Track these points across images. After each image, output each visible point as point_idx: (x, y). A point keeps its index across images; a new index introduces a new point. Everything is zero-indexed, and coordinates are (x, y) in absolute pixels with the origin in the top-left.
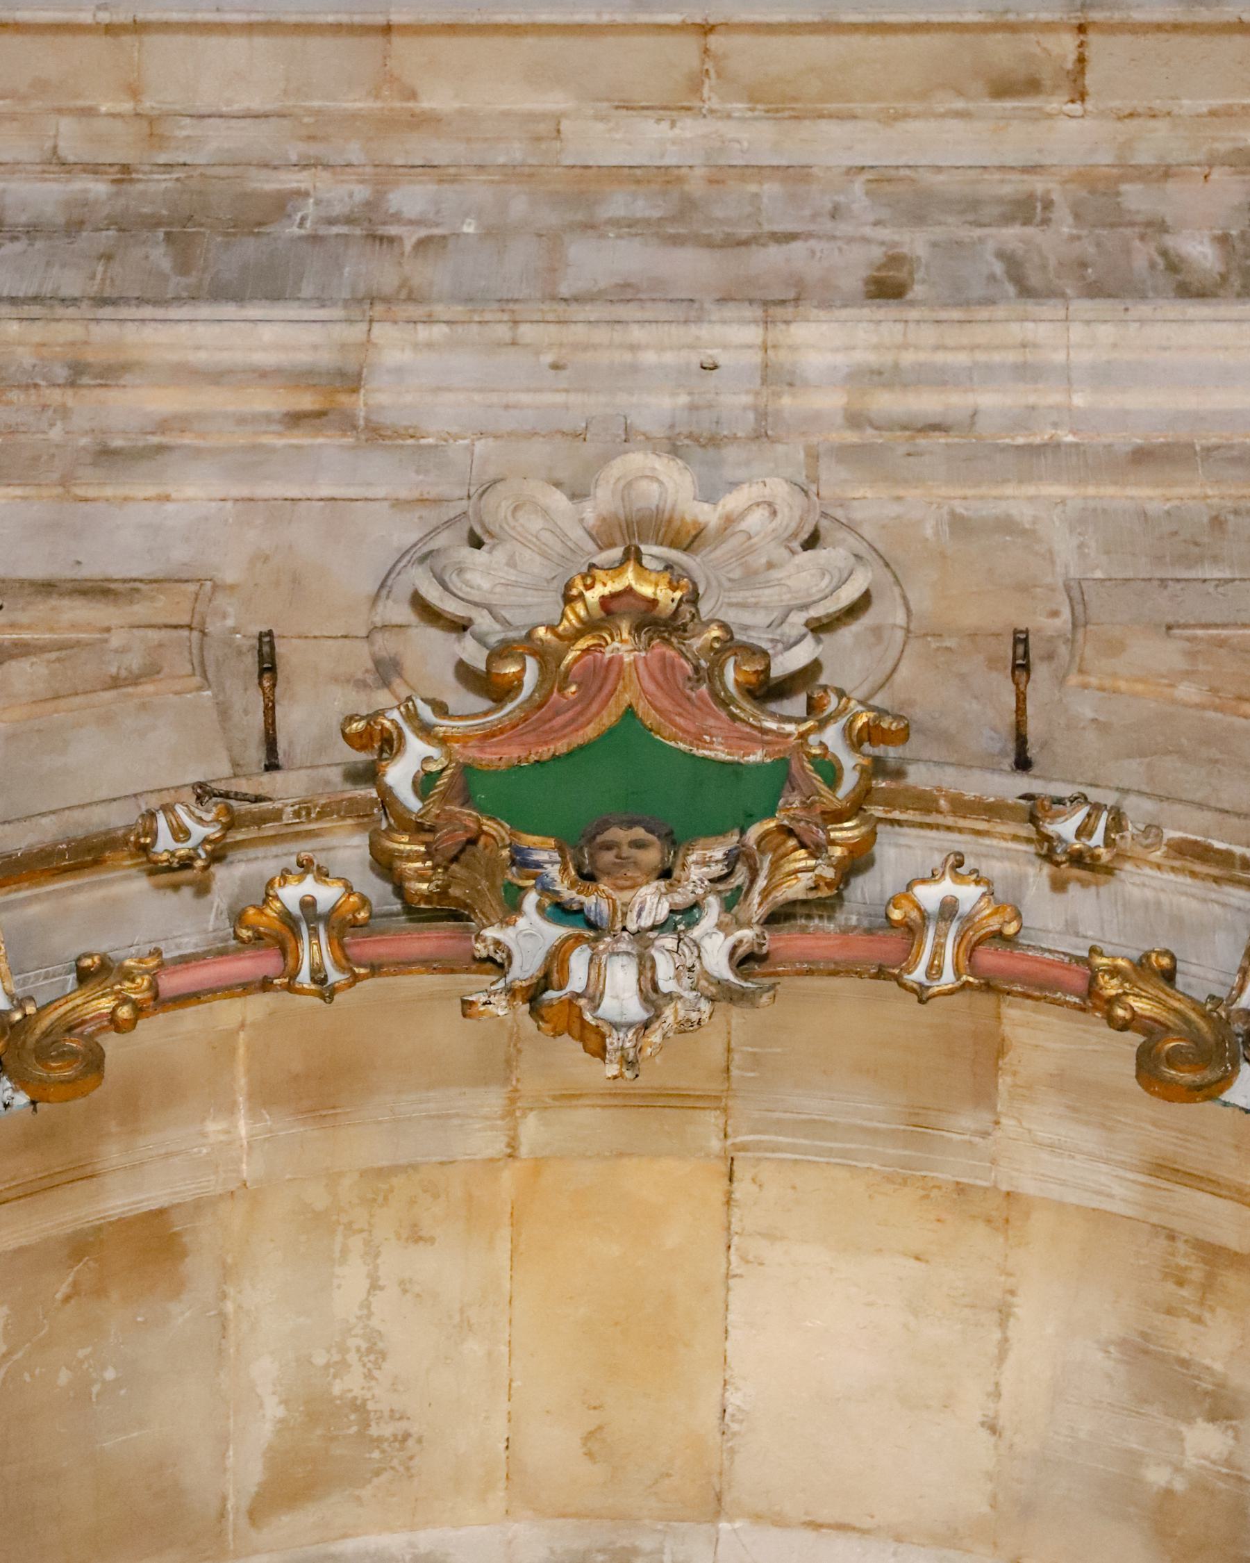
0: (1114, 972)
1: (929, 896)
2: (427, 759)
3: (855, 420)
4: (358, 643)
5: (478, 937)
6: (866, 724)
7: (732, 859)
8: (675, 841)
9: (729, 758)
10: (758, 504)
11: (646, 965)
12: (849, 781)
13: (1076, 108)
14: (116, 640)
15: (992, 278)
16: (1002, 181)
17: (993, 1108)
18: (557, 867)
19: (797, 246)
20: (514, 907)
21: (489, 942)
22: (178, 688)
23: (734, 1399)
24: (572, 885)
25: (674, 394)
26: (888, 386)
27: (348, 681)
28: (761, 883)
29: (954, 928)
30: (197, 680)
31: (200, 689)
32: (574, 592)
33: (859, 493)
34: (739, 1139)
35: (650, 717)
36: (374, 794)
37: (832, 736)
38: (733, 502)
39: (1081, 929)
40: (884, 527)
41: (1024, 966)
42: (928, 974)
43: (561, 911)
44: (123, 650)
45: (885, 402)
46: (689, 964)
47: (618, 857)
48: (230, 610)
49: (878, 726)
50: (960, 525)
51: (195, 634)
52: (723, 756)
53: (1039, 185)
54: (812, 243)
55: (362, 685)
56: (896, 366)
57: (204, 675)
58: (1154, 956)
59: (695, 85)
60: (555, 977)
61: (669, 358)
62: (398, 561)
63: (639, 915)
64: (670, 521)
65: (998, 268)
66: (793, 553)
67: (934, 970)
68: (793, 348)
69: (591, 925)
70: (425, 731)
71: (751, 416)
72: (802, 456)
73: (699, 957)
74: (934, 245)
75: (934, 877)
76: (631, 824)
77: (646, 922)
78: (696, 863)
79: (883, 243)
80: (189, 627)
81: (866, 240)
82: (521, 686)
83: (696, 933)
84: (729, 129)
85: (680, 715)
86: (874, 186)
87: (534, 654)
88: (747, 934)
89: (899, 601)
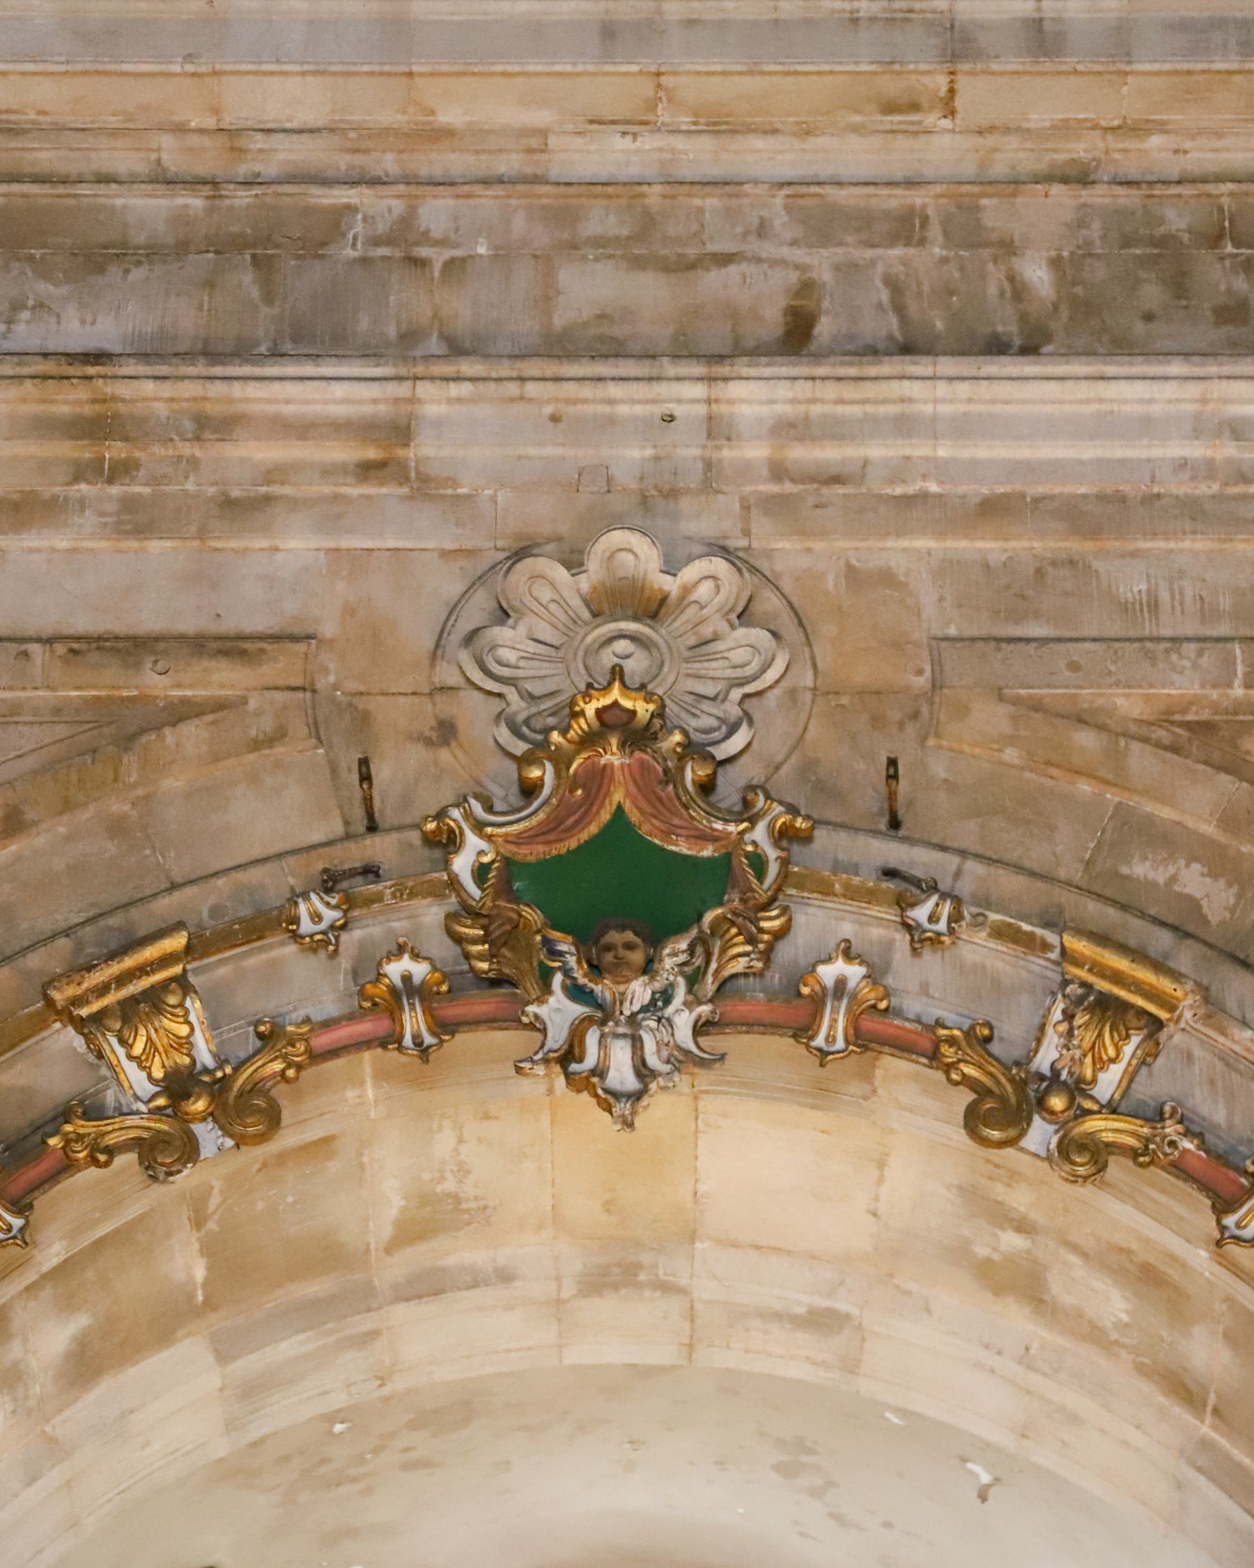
0: (952, 1041)
1: (828, 973)
2: (481, 853)
3: (778, 471)
4: (423, 698)
5: (523, 1012)
6: (784, 823)
7: (691, 950)
8: (655, 939)
9: (689, 853)
10: (706, 578)
11: (637, 1043)
12: (773, 870)
13: (946, 123)
14: (253, 704)
15: (880, 305)
16: (890, 196)
17: (872, 1083)
18: (574, 958)
19: (733, 269)
20: (547, 989)
21: (531, 1014)
22: (300, 748)
23: (702, 1188)
24: (585, 975)
25: (644, 447)
26: (801, 439)
27: (419, 739)
28: (713, 966)
29: (845, 1002)
30: (314, 740)
31: (316, 748)
32: (577, 709)
33: (780, 545)
34: (703, 1088)
35: (634, 816)
36: (446, 878)
37: (760, 833)
38: (690, 573)
39: (931, 991)
40: (798, 579)
41: (891, 1031)
42: (827, 1039)
43: (576, 992)
44: (258, 713)
45: (798, 453)
46: (666, 1040)
47: (616, 957)
48: (331, 666)
49: (793, 827)
50: (854, 576)
51: (308, 694)
52: (685, 851)
53: (918, 198)
54: (744, 267)
55: (428, 742)
56: (807, 418)
57: (319, 738)
58: (978, 1028)
59: (652, 106)
60: (577, 1051)
61: (639, 410)
62: (447, 619)
63: (631, 1003)
64: (643, 589)
65: (885, 296)
66: (733, 627)
67: (830, 1039)
68: (731, 402)
69: (600, 1006)
70: (479, 826)
71: (700, 465)
72: (737, 507)
73: (673, 1035)
74: (837, 268)
75: (829, 960)
76: (623, 928)
77: (636, 1008)
78: (669, 955)
79: (797, 267)
80: (304, 689)
81: (783, 263)
82: (542, 786)
83: (669, 1011)
84: (679, 143)
85: (655, 817)
86: (791, 200)
87: (550, 759)
88: (705, 1009)
89: (809, 663)
